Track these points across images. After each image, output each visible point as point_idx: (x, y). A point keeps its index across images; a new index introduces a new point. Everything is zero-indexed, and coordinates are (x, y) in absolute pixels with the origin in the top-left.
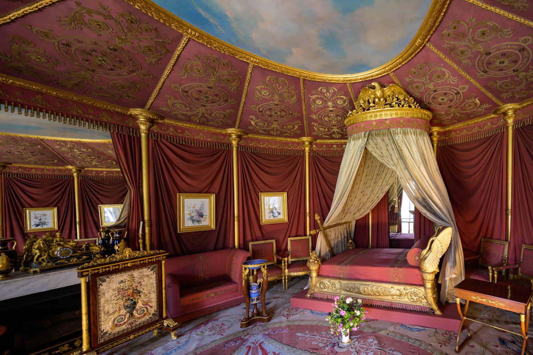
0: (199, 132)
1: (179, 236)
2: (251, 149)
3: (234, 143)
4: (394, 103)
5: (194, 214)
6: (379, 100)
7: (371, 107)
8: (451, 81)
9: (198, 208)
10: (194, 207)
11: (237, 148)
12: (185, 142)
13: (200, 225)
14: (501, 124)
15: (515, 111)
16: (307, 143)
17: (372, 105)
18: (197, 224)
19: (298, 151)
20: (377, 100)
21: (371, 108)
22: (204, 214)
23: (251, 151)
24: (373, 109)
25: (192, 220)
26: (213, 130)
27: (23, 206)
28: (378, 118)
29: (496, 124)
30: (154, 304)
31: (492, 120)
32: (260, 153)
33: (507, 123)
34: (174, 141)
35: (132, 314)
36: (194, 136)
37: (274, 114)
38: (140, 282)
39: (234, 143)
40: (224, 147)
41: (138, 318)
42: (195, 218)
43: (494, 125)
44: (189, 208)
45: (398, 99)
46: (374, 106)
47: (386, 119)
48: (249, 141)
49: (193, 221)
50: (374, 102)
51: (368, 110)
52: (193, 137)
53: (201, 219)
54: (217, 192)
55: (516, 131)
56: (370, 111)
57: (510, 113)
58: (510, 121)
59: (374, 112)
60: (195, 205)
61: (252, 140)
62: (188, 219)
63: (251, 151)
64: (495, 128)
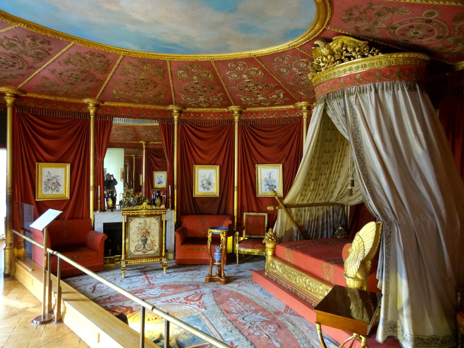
0: (210, 113)
1: (194, 199)
2: (250, 122)
3: (236, 118)
5: (205, 182)
9: (207, 177)
10: (204, 176)
11: (239, 123)
12: (200, 123)
13: (209, 191)
16: (305, 108)
18: (206, 191)
19: (295, 118)
22: (212, 183)
23: (250, 124)
25: (203, 187)
26: (218, 110)
27: (153, 170)
30: (157, 243)
32: (258, 125)
34: (193, 124)
35: (144, 246)
36: (207, 117)
37: (255, 87)
38: (150, 227)
39: (236, 118)
40: (227, 123)
41: (148, 250)
42: (205, 186)
44: (201, 177)
47: (339, 78)
48: (249, 115)
49: (204, 188)
52: (206, 118)
53: (210, 187)
54: (221, 164)
60: (205, 174)
61: (252, 113)
62: (200, 186)
63: (250, 124)
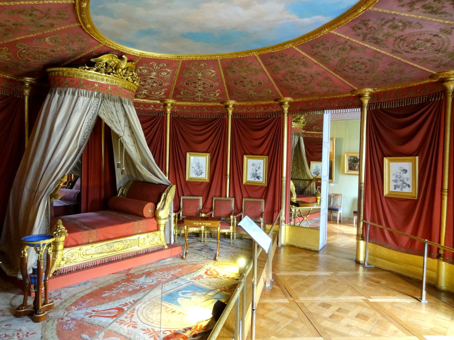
4: (129, 78)
6: (122, 70)
7: (113, 73)
8: (166, 79)
14: (161, 110)
15: (172, 105)
17: (114, 71)
20: (120, 70)
21: (112, 74)
24: (113, 75)
28: (114, 84)
29: (158, 109)
31: (155, 105)
33: (166, 111)
43: (157, 108)
45: (133, 75)
46: (115, 74)
50: (116, 69)
51: (109, 74)
55: (172, 119)
56: (111, 76)
57: (169, 105)
58: (169, 110)
59: (112, 78)
64: (157, 111)
